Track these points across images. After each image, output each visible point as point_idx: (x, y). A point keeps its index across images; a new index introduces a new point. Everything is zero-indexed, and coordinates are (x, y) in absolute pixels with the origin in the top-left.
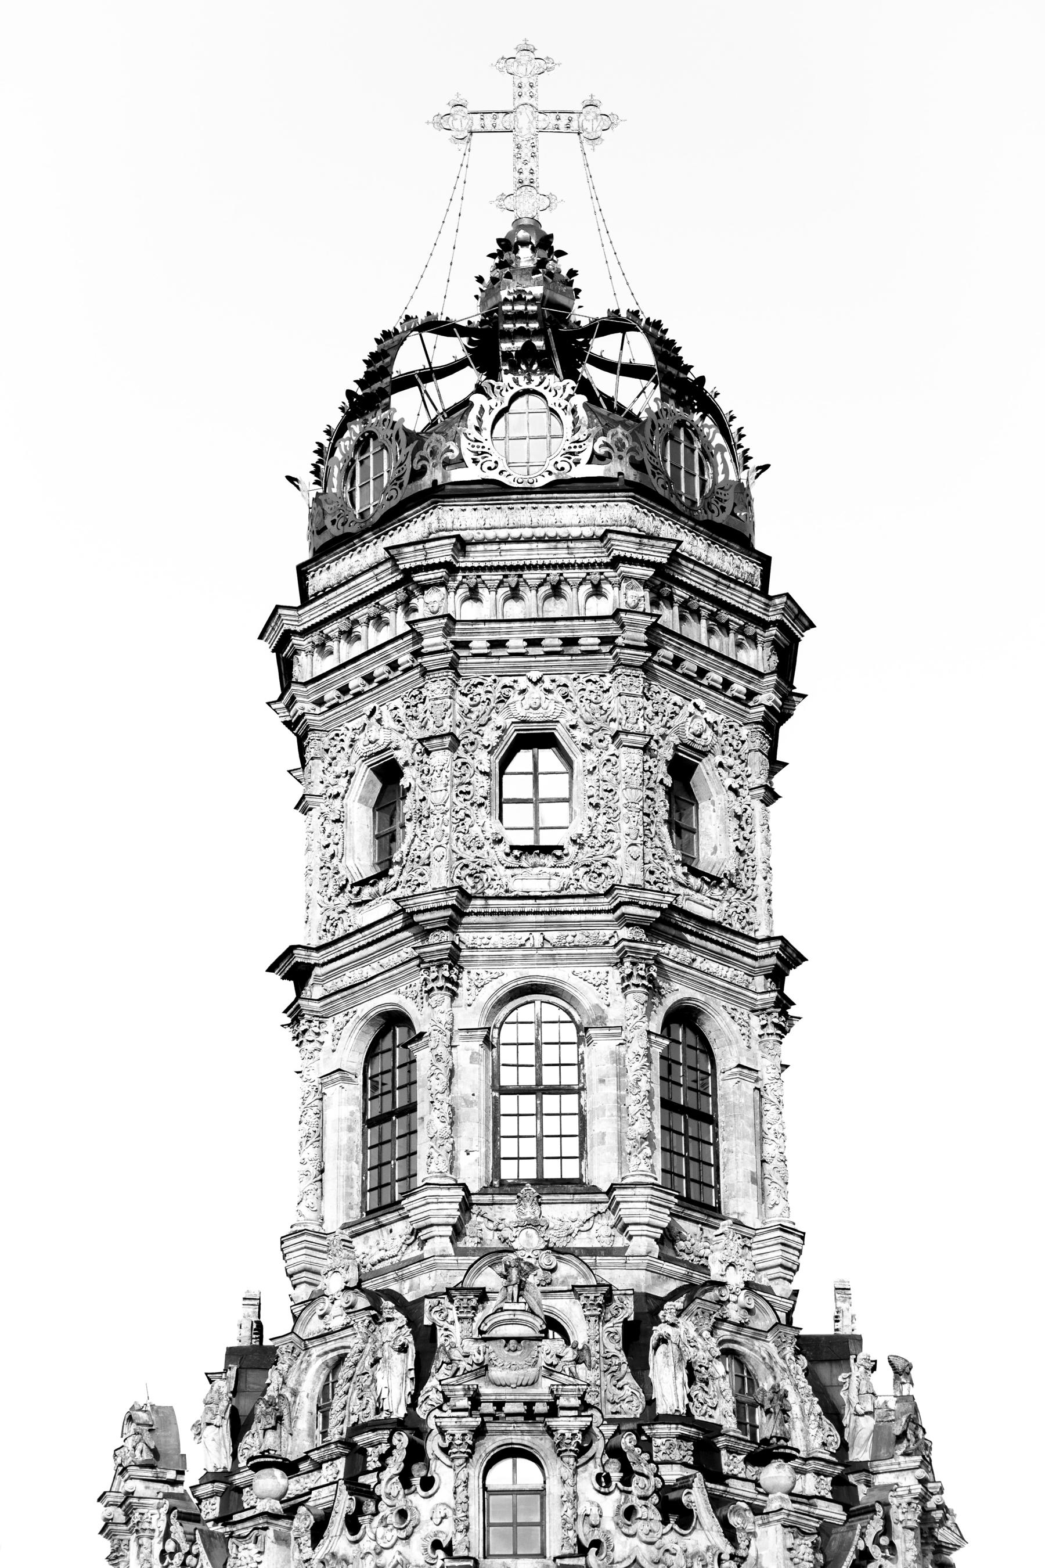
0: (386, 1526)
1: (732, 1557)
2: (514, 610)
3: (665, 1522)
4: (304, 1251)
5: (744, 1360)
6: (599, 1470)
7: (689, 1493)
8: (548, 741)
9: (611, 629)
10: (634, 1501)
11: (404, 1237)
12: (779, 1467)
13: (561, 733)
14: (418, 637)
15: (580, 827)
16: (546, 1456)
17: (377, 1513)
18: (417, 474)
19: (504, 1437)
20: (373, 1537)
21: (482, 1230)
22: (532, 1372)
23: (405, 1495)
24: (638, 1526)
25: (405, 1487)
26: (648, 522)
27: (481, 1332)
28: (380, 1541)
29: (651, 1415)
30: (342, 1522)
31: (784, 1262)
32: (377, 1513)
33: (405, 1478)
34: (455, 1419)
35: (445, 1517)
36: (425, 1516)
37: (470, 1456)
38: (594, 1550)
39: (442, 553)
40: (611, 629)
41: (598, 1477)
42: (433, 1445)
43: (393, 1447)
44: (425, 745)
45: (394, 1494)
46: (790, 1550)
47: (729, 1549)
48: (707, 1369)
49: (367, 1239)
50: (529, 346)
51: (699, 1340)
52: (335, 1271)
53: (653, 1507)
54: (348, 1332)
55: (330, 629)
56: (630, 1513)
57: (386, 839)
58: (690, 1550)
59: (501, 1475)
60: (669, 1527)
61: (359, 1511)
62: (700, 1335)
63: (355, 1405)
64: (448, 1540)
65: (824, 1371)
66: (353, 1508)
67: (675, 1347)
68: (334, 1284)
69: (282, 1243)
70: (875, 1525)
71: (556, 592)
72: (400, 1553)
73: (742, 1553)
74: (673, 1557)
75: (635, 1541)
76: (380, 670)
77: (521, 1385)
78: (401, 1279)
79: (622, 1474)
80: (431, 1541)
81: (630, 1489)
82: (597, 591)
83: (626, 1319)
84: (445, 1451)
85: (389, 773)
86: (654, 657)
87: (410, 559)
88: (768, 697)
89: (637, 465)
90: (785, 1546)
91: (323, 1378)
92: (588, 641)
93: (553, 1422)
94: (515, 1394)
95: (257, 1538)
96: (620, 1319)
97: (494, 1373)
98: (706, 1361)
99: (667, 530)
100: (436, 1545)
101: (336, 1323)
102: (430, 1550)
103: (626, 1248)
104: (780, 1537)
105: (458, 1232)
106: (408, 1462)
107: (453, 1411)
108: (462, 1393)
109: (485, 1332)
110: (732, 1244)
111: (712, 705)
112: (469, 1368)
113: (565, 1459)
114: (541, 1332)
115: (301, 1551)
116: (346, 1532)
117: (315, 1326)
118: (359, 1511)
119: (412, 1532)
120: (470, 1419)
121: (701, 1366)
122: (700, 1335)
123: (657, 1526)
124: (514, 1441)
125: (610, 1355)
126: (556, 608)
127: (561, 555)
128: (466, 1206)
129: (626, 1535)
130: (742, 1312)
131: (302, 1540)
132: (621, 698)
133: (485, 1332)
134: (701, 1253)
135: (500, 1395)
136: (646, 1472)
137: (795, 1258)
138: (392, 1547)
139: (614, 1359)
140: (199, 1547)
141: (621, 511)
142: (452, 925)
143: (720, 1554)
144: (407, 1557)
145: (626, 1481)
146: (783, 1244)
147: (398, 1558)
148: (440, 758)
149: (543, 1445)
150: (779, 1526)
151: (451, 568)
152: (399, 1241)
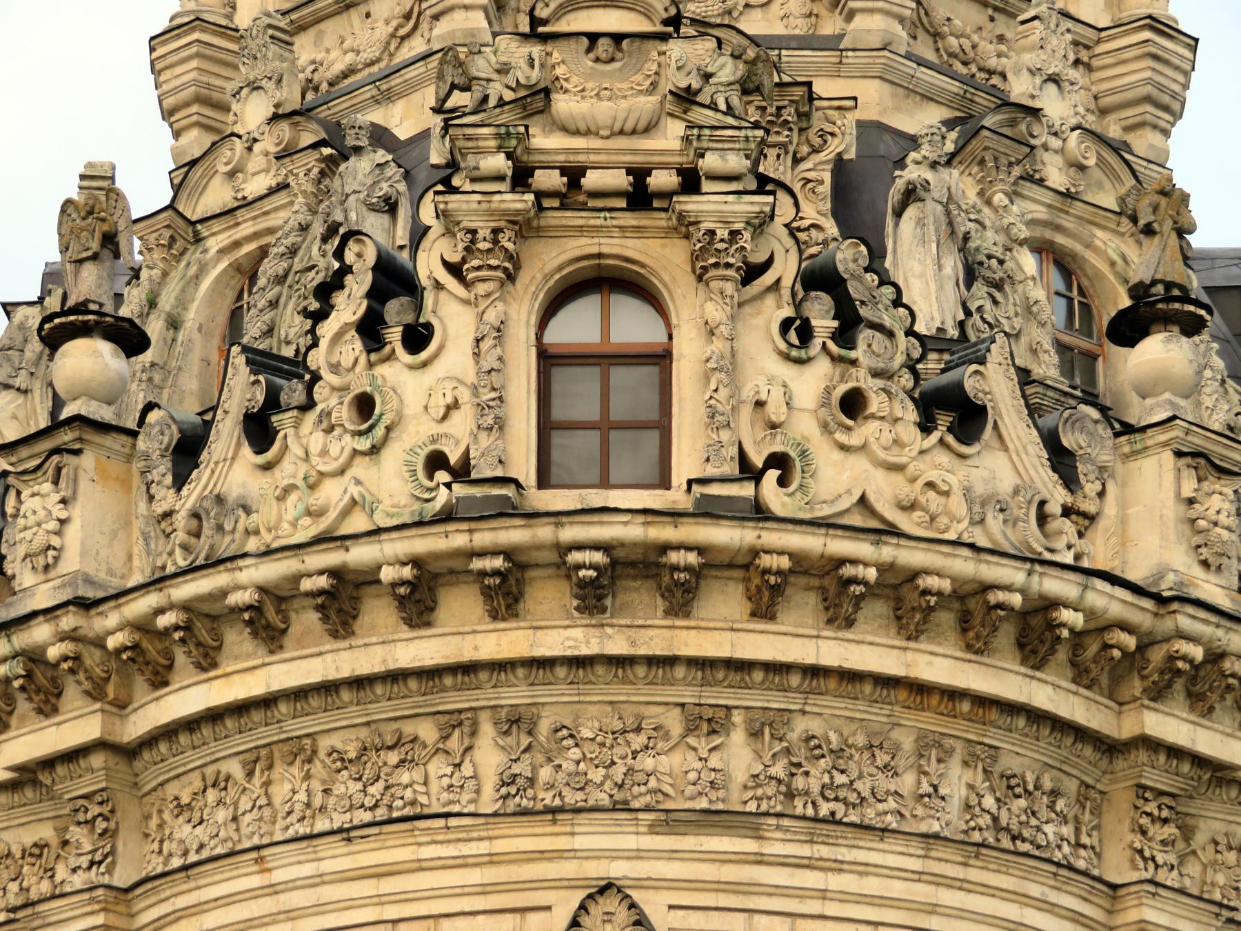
0: (330, 429)
1: (1067, 512)
3: (926, 427)
4: (194, 63)
5: (1073, 267)
6: (788, 312)
7: (977, 372)
10: (861, 379)
11: (394, 23)
12: (1168, 340)
16: (674, 279)
17: (309, 405)
19: (584, 241)
20: (301, 453)
22: (648, 103)
23: (371, 365)
24: (867, 431)
25: (369, 352)
27: (535, 22)
28: (315, 460)
30: (238, 430)
31: (1155, 93)
32: (309, 405)
33: (370, 330)
34: (477, 197)
35: (455, 405)
36: (413, 405)
37: (511, 277)
38: (772, 475)
41: (786, 325)
43: (345, 270)
45: (347, 361)
46: (1191, 502)
47: (1058, 496)
48: (1001, 262)
49: (320, 34)
51: (986, 210)
52: (255, 87)
53: (902, 395)
54: (281, 199)
56: (853, 404)
58: (979, 490)
59: (578, 325)
60: (935, 437)
61: (273, 403)
62: (989, 203)
64: (461, 449)
66: (260, 397)
67: (939, 208)
68: (253, 113)
69: (152, 50)
72: (358, 482)
73: (1089, 507)
74: (942, 500)
75: (859, 463)
77: (621, 132)
78: (386, 98)
79: (836, 324)
80: (423, 453)
81: (853, 354)
83: (839, 154)
84: (455, 270)
90: (1178, 494)
91: (231, 295)
93: (690, 204)
94: (607, 151)
95: (59, 470)
96: (828, 154)
97: (563, 105)
98: (1000, 250)
100: (436, 461)
101: (256, 186)
102: (421, 474)
103: (841, 36)
104: (1169, 478)
106: (378, 296)
107: (474, 180)
108: (493, 143)
109: (545, 22)
110: (1054, 41)
112: (509, 96)
113: (715, 285)
114: (666, 22)
115: (151, 498)
116: (247, 450)
117: (216, 196)
118: (273, 403)
119: (386, 439)
120: (509, 197)
121: (989, 257)
122: (989, 203)
123: (909, 432)
124: (605, 250)
125: (806, 223)
129: (843, 448)
130: (1072, 171)
131: (155, 475)
133: (545, 22)
134: (993, 63)
135: (576, 151)
136: (887, 322)
137: (1176, 88)
138: (342, 472)
139: (813, 232)
143: (1042, 503)
144: (373, 489)
145: (846, 333)
146: (1155, 57)
147: (354, 491)
149: (664, 259)
150: (1168, 456)
152: (383, 31)
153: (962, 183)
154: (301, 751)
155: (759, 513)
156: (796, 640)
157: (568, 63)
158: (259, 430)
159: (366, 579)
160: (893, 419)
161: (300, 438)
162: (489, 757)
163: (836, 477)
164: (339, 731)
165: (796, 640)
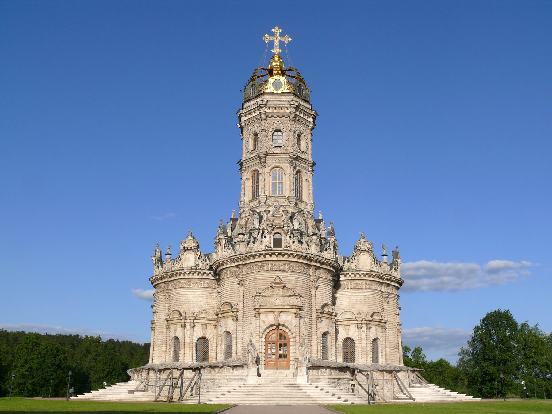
2: (275, 111)
8: (279, 131)
9: (290, 114)
13: (282, 130)
14: (261, 115)
15: (284, 144)
18: (261, 91)
21: (269, 202)
26: (295, 99)
29: (294, 229)
33: (262, 236)
39: (265, 102)
40: (290, 114)
42: (266, 232)
44: (262, 131)
50: (278, 72)
55: (247, 113)
57: (255, 145)
63: (250, 227)
65: (317, 224)
68: (247, 209)
70: (328, 245)
71: (281, 109)
76: (255, 119)
82: (287, 109)
85: (256, 135)
86: (295, 119)
87: (260, 103)
88: (311, 125)
89: (294, 90)
92: (286, 116)
99: (298, 100)
101: (247, 215)
105: (265, 202)
111: (304, 126)
126: (281, 111)
127: (282, 103)
128: (267, 198)
132: (290, 125)
140: (230, 246)
141: (291, 97)
142: (265, 157)
148: (264, 133)
149: (282, 232)
151: (266, 105)
153: (299, 217)
154: (256, 265)
155: (288, 250)
156: (291, 259)
157: (275, 219)
158: (254, 242)
159: (261, 254)
160: (297, 242)
161: (256, 243)
162: (269, 267)
163: (293, 247)
164: (259, 264)
165: (291, 259)
